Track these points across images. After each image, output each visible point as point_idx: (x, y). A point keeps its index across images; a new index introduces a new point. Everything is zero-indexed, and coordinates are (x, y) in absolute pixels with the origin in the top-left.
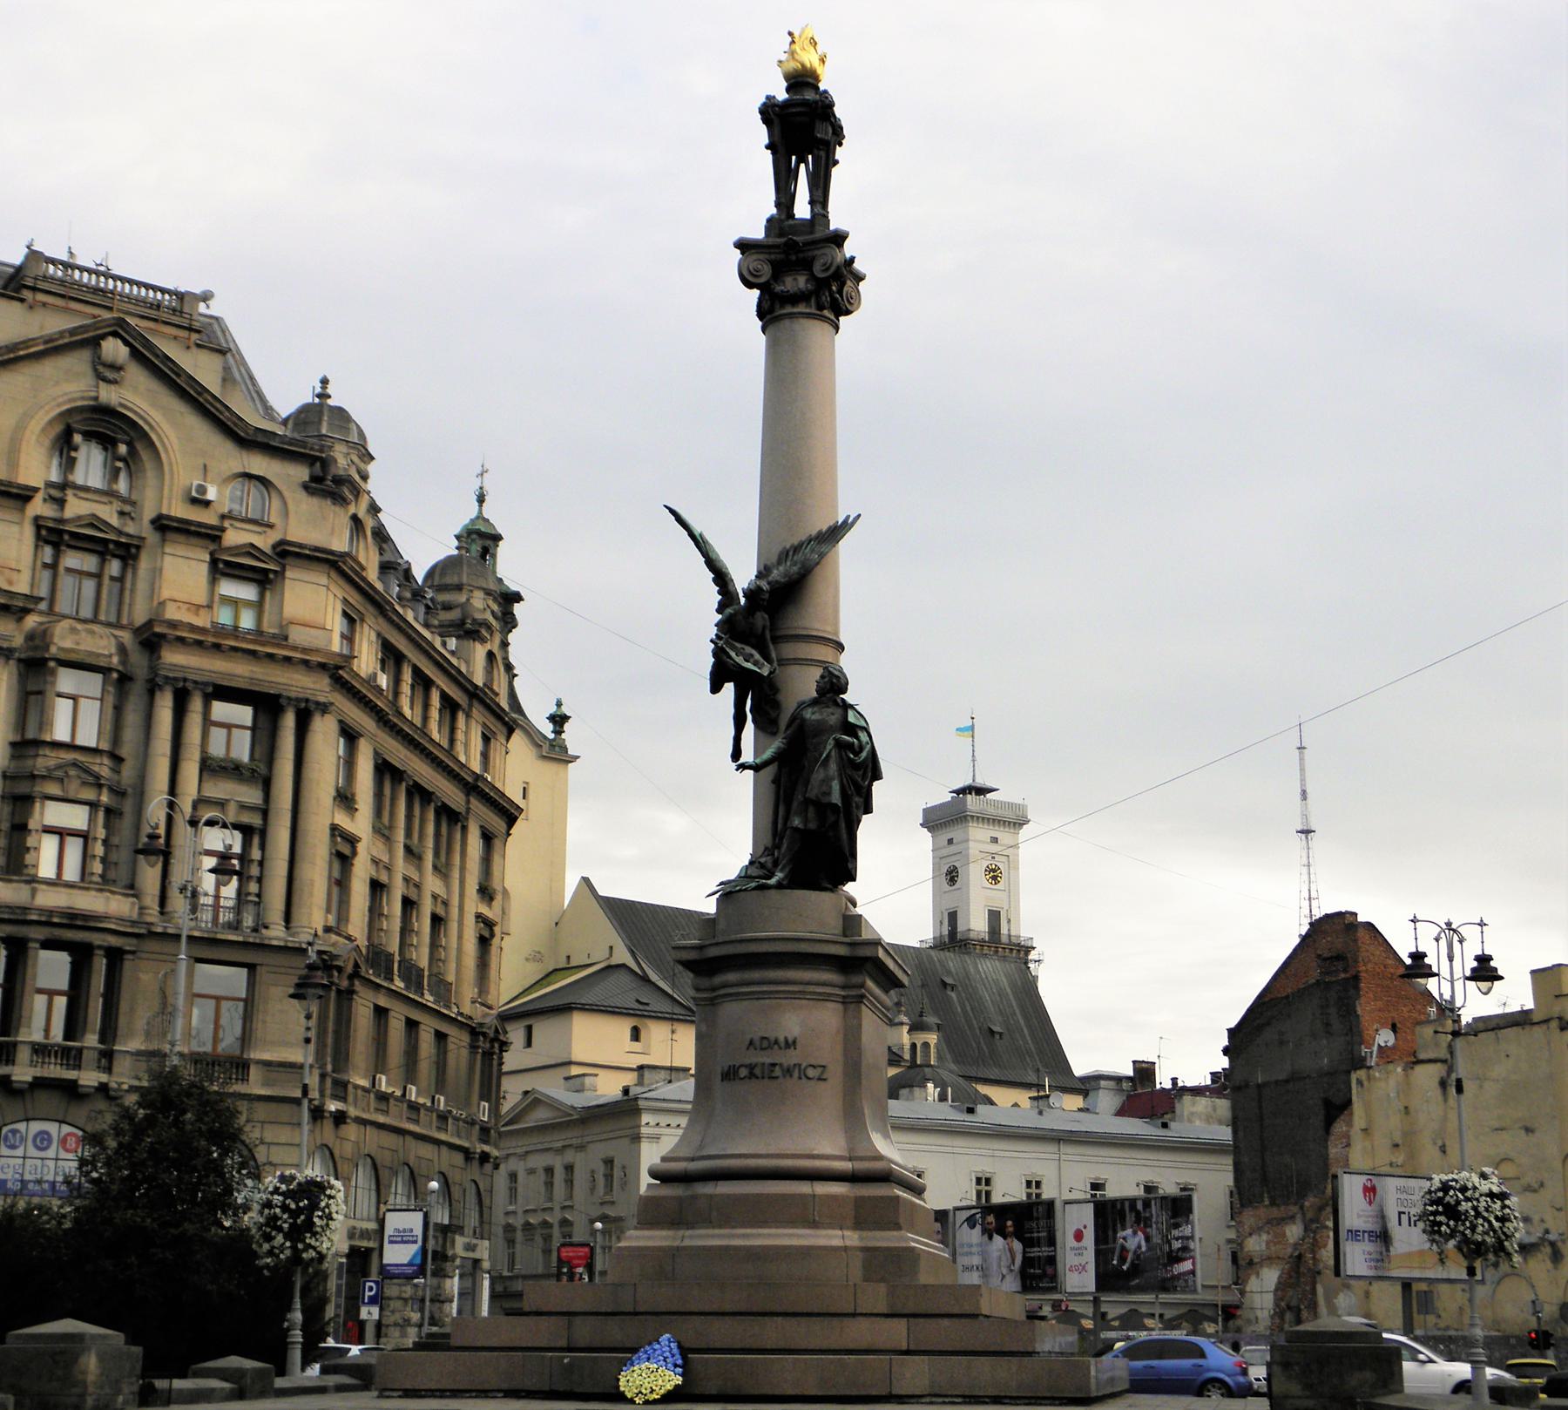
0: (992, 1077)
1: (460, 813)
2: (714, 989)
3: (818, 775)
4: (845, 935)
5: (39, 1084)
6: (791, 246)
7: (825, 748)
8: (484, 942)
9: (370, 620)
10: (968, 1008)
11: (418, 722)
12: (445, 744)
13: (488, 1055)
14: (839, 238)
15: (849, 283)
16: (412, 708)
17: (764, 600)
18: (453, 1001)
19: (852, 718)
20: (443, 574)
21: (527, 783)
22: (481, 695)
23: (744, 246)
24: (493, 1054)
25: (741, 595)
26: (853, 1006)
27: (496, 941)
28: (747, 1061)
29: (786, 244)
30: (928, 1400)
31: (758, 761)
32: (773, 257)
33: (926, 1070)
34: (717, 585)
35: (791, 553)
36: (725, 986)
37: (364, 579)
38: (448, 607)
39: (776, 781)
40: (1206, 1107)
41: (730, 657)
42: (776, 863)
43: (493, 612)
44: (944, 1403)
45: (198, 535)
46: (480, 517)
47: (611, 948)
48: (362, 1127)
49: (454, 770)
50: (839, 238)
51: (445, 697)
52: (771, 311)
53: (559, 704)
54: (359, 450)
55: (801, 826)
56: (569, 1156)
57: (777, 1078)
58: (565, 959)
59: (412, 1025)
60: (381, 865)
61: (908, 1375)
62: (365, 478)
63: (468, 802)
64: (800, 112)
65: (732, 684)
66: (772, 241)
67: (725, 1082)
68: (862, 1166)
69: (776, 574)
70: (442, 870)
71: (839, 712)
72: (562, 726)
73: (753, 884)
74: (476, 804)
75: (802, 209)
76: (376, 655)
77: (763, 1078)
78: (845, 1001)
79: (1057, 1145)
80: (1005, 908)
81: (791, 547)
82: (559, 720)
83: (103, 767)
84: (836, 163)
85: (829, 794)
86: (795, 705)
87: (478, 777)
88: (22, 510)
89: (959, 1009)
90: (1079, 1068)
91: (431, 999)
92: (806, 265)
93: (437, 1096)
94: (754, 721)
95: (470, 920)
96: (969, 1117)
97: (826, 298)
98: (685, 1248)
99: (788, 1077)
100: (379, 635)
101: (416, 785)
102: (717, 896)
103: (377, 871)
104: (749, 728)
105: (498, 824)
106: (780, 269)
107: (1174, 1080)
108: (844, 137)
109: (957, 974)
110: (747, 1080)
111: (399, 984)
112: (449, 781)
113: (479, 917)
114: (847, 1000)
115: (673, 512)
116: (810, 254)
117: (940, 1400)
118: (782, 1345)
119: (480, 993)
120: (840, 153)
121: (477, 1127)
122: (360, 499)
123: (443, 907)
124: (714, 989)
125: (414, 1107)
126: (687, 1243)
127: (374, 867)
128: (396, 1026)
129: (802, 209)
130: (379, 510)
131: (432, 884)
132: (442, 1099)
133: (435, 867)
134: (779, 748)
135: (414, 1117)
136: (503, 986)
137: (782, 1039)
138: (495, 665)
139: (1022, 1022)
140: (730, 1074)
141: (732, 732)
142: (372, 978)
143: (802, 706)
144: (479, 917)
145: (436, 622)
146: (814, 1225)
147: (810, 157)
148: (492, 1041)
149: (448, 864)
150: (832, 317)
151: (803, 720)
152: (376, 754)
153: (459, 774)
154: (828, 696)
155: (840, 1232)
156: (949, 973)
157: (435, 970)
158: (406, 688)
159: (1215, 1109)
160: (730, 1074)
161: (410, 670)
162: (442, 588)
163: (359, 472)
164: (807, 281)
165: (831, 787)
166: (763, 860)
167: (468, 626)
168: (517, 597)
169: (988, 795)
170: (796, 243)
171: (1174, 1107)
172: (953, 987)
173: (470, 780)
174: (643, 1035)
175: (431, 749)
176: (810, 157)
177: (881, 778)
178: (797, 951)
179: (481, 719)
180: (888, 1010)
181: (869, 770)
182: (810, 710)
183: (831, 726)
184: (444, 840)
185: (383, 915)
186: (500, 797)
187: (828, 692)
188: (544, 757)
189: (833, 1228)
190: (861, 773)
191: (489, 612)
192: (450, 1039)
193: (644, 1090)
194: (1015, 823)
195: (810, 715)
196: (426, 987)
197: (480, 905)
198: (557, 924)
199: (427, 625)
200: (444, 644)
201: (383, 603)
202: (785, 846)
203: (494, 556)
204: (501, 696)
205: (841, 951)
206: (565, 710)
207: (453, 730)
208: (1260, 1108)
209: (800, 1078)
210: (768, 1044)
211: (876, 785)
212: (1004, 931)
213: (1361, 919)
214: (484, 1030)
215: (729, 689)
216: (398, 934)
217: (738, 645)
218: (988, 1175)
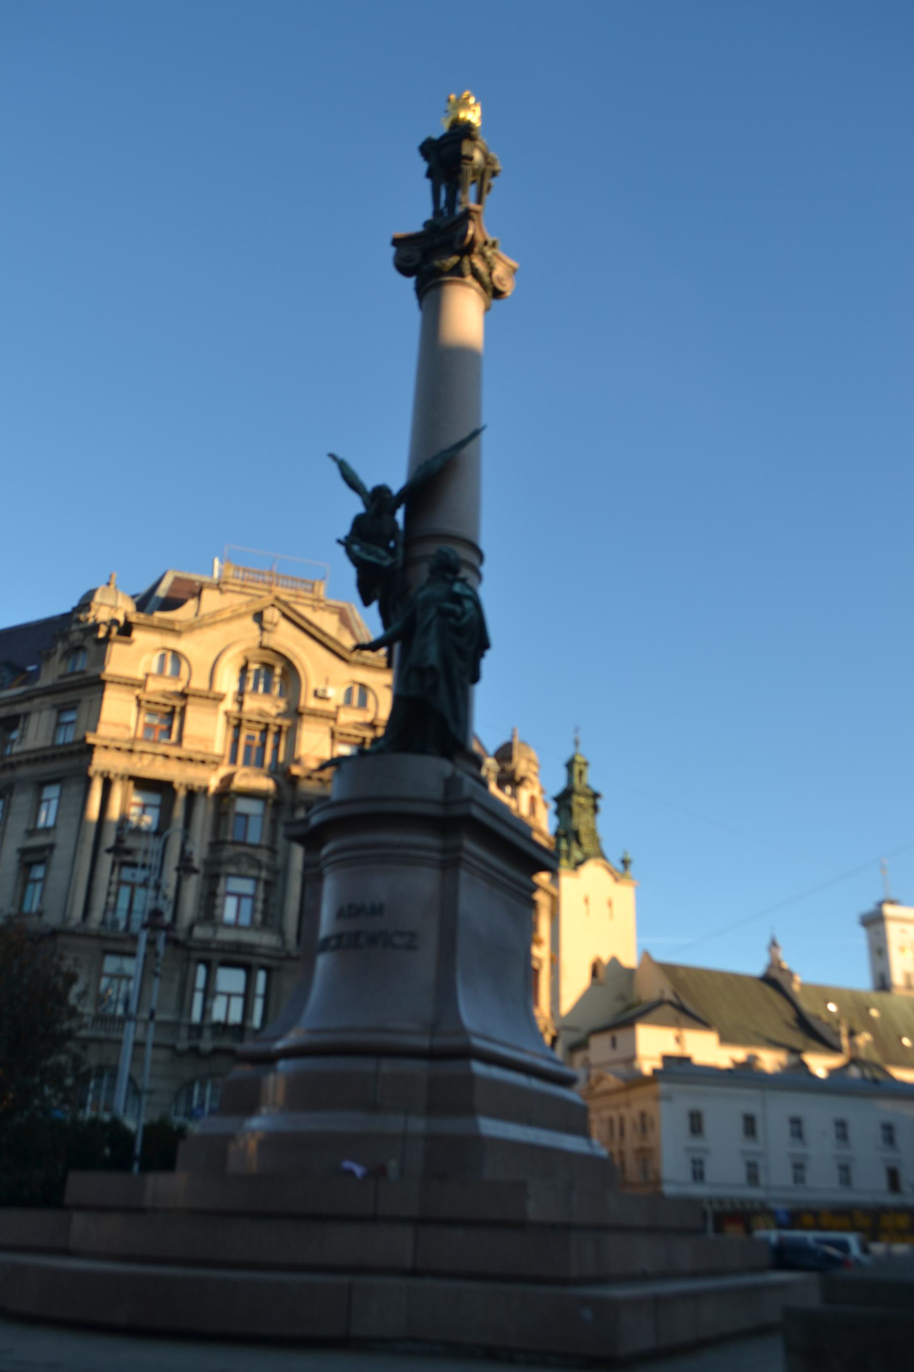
5: (216, 1052)
45: (321, 716)
56: (624, 1111)
68: (440, 1042)
83: (263, 856)
88: (216, 707)
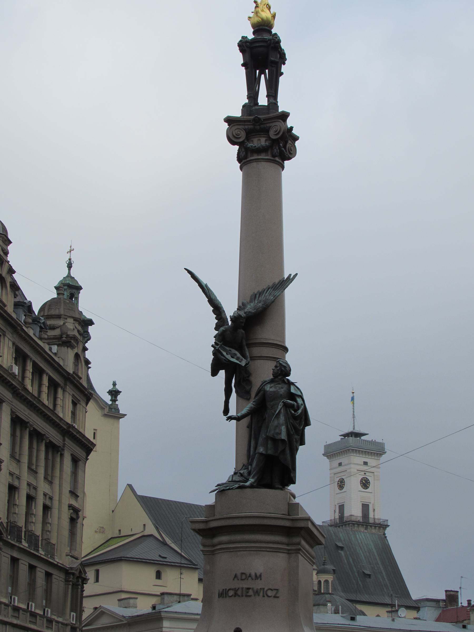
0: (364, 600)
1: (59, 447)
2: (214, 546)
4: (289, 515)
6: (257, 121)
7: (278, 407)
8: (73, 521)
9: (9, 335)
10: (351, 560)
11: (36, 394)
12: (51, 407)
13: (75, 586)
14: (285, 116)
15: (290, 142)
16: (32, 386)
18: (56, 554)
19: (293, 390)
20: (50, 309)
21: (96, 430)
22: (72, 378)
23: (229, 120)
24: (78, 585)
25: (229, 319)
27: (80, 520)
28: (233, 587)
29: (254, 120)
31: (239, 415)
32: (246, 127)
33: (327, 596)
34: (215, 314)
35: (257, 296)
36: (220, 543)
37: (6, 312)
38: (53, 328)
39: (250, 426)
41: (223, 355)
42: (249, 473)
43: (78, 331)
46: (69, 276)
47: (144, 525)
48: (4, 626)
49: (56, 422)
50: (285, 116)
51: (51, 380)
52: (246, 157)
53: (114, 384)
54: (3, 238)
55: (264, 452)
57: (250, 596)
58: (118, 532)
59: (32, 568)
60: (15, 476)
62: (6, 253)
63: (64, 440)
65: (224, 370)
66: (246, 118)
67: (221, 598)
69: (250, 308)
70: (49, 480)
71: (285, 387)
72: (116, 397)
73: (237, 486)
74: (68, 441)
75: (263, 100)
76: (12, 355)
77: (242, 596)
78: (289, 552)
80: (372, 503)
81: (258, 292)
82: (114, 393)
84: (282, 74)
85: (280, 434)
86: (261, 383)
87: (70, 426)
89: (346, 561)
90: (415, 595)
91: (43, 553)
92: (266, 131)
93: (46, 609)
94: (236, 392)
95: (65, 508)
96: (352, 623)
97: (276, 151)
100: (14, 344)
101: (35, 430)
102: (216, 492)
103: (13, 480)
104: (234, 395)
105: (80, 452)
106: (250, 134)
107: (469, 601)
108: (286, 60)
109: (344, 540)
111: (25, 544)
112: (53, 428)
113: (71, 507)
114: (290, 552)
115: (189, 272)
116: (268, 125)
119: (71, 549)
120: (284, 69)
121: (69, 627)
122: (3, 265)
123: (50, 501)
124: (214, 546)
125: (33, 615)
127: (11, 477)
128: (23, 568)
129: (263, 100)
130: (14, 272)
131: (43, 487)
132: (49, 610)
133: (45, 478)
134: (251, 407)
135: (34, 621)
136: (84, 546)
137: (253, 574)
138: (79, 362)
139: (382, 568)
140: (223, 594)
142: (10, 541)
143: (265, 383)
144: (70, 506)
145: (46, 337)
147: (267, 71)
148: (78, 578)
149: (52, 477)
150: (280, 161)
151: (265, 392)
152: (12, 412)
153: (59, 424)
154: (280, 377)
156: (340, 540)
157: (45, 537)
158: (29, 374)
160: (223, 594)
161: (31, 363)
162: (49, 317)
163: (3, 250)
164: (266, 140)
165: (281, 430)
166: (242, 472)
167: (64, 338)
168: (90, 322)
169: (363, 438)
170: (259, 119)
171: (469, 617)
172: (342, 548)
173: (65, 427)
174: (163, 575)
175: (44, 410)
176: (267, 71)
179: (72, 392)
180: (313, 558)
181: (303, 420)
182: (269, 386)
183: (281, 395)
184: (50, 463)
185: (16, 505)
186: (83, 438)
187: (280, 375)
188: (106, 415)
190: (298, 422)
191: (76, 331)
192: (54, 577)
193: (166, 606)
194: (377, 454)
195: (268, 388)
196: (40, 546)
197: (71, 499)
198: (113, 511)
199: (41, 339)
200: (50, 349)
201: (16, 325)
202: (254, 465)
203: (77, 299)
204: (83, 379)
205: (288, 524)
206: (118, 387)
207: (55, 399)
209: (264, 596)
210: (245, 576)
211: (307, 429)
212: (371, 515)
214: (73, 571)
215: (222, 373)
216: (24, 516)
217: (228, 348)
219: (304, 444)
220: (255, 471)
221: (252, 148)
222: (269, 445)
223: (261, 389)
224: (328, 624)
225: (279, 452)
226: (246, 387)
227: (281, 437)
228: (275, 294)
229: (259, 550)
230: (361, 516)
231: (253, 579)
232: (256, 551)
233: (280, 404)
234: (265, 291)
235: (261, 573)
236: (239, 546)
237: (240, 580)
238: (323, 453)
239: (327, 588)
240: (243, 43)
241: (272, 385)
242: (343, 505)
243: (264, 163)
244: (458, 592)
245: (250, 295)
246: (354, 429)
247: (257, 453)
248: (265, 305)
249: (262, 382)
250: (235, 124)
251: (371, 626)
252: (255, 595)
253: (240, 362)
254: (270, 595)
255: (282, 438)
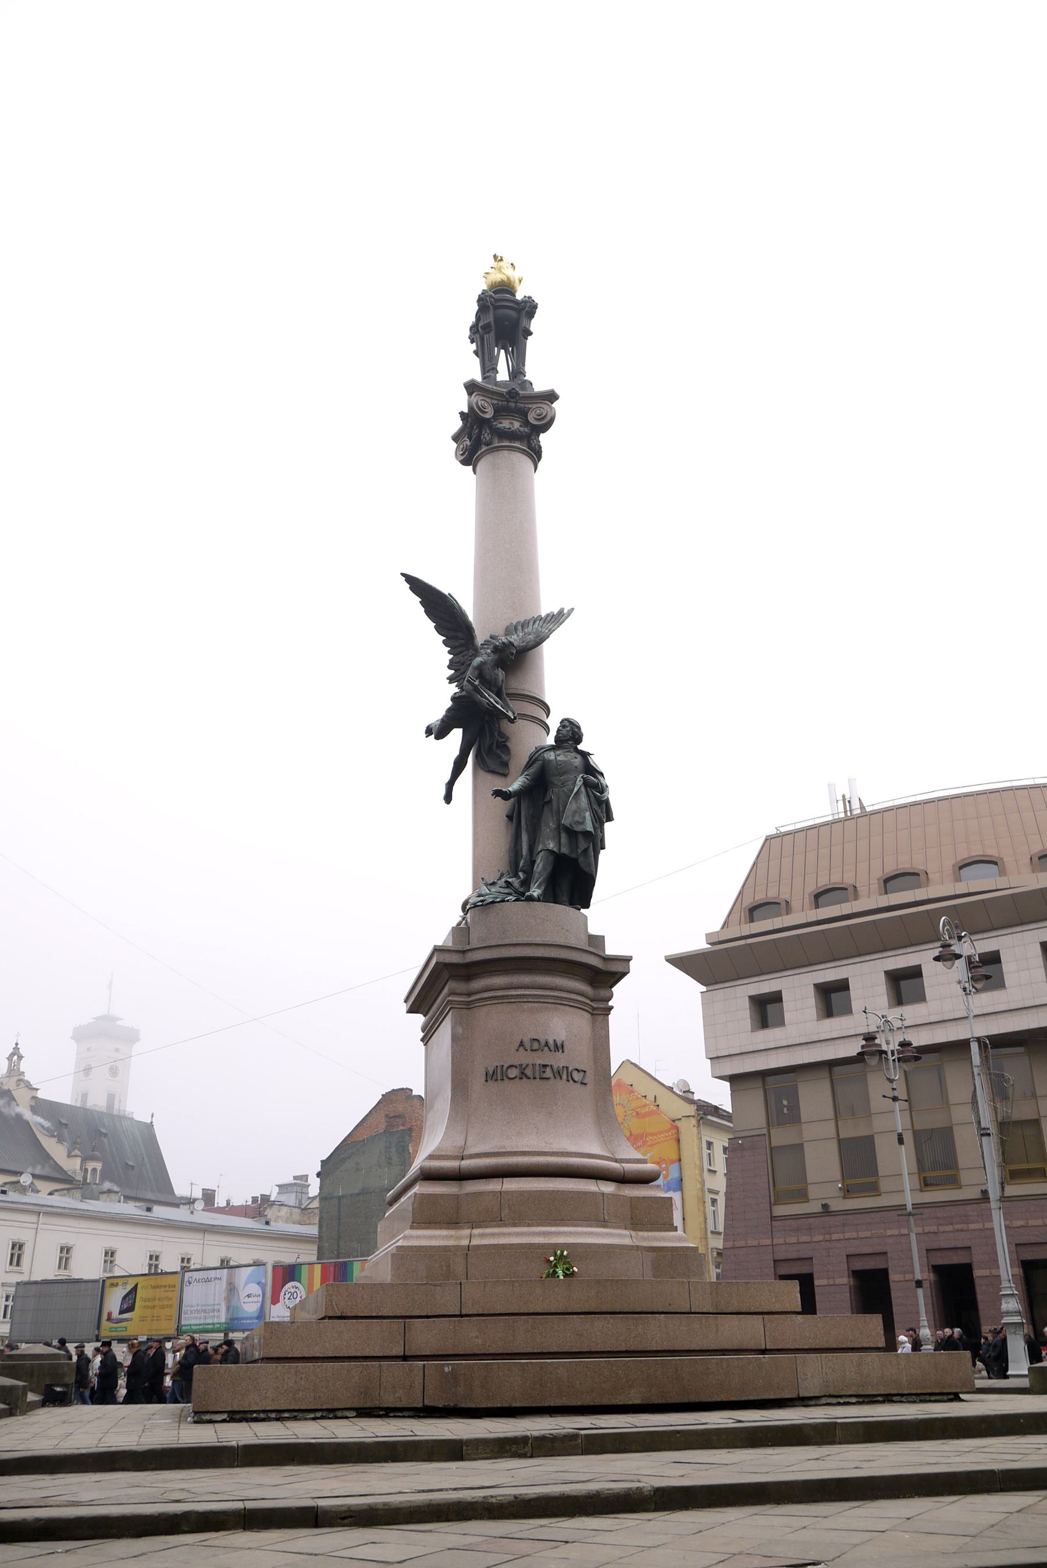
3: (571, 806)
10: (114, 1149)
17: (512, 654)
23: (471, 387)
26: (601, 1018)
29: (509, 393)
30: (824, 1401)
32: (496, 402)
35: (520, 627)
40: (287, 1212)
44: (839, 1404)
55: (555, 850)
61: (809, 1375)
64: (513, 307)
65: (461, 729)
67: (490, 1082)
71: (579, 756)
79: (202, 1236)
81: (518, 623)
85: (582, 823)
89: (108, 1149)
92: (523, 414)
96: (148, 1214)
98: (478, 1247)
99: (558, 1077)
106: (499, 412)
107: (228, 1202)
110: (517, 1080)
114: (595, 1012)
117: (834, 1401)
118: (666, 1346)
124: (469, 995)
126: (475, 1242)
134: (525, 782)
137: (551, 1042)
140: (495, 1075)
141: (447, 777)
146: (603, 1223)
155: (626, 1232)
159: (291, 1215)
160: (495, 1075)
165: (585, 818)
169: (118, 1022)
170: (517, 394)
172: (105, 1135)
177: (613, 820)
178: (570, 958)
183: (576, 767)
189: (620, 1228)
195: (551, 756)
208: (339, 1211)
210: (538, 1045)
212: (116, 1106)
213: (414, 1093)
215: (456, 735)
218: (157, 1254)
219: (604, 848)
220: (542, 878)
221: (506, 430)
222: (562, 840)
223: (538, 757)
224: (122, 1214)
225: (580, 851)
226: (503, 756)
227: (584, 827)
228: (550, 627)
229: (559, 1002)
230: (106, 1106)
231: (551, 1051)
232: (554, 1003)
233: (578, 779)
234: (531, 623)
235: (563, 1041)
236: (528, 993)
237: (529, 1050)
238: (71, 1035)
239: (94, 1178)
240: (487, 296)
241: (558, 752)
242: (87, 1093)
243: (520, 455)
244: (215, 1191)
245: (505, 627)
246: (108, 1012)
247: (541, 851)
248: (540, 638)
249: (536, 748)
250: (480, 393)
251: (170, 1219)
252: (555, 1078)
253: (507, 712)
254: (576, 1079)
255: (588, 830)
